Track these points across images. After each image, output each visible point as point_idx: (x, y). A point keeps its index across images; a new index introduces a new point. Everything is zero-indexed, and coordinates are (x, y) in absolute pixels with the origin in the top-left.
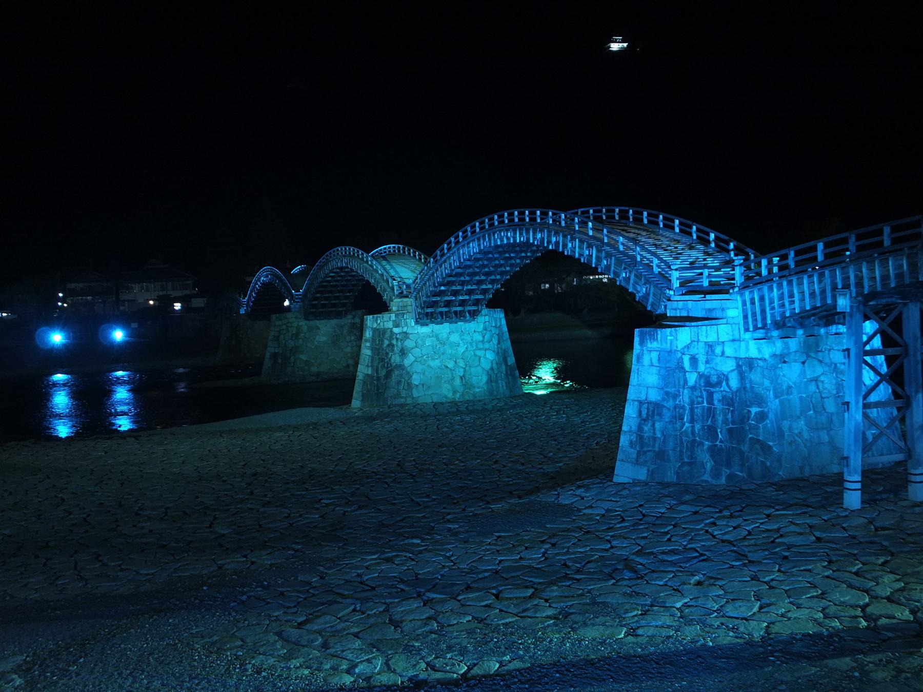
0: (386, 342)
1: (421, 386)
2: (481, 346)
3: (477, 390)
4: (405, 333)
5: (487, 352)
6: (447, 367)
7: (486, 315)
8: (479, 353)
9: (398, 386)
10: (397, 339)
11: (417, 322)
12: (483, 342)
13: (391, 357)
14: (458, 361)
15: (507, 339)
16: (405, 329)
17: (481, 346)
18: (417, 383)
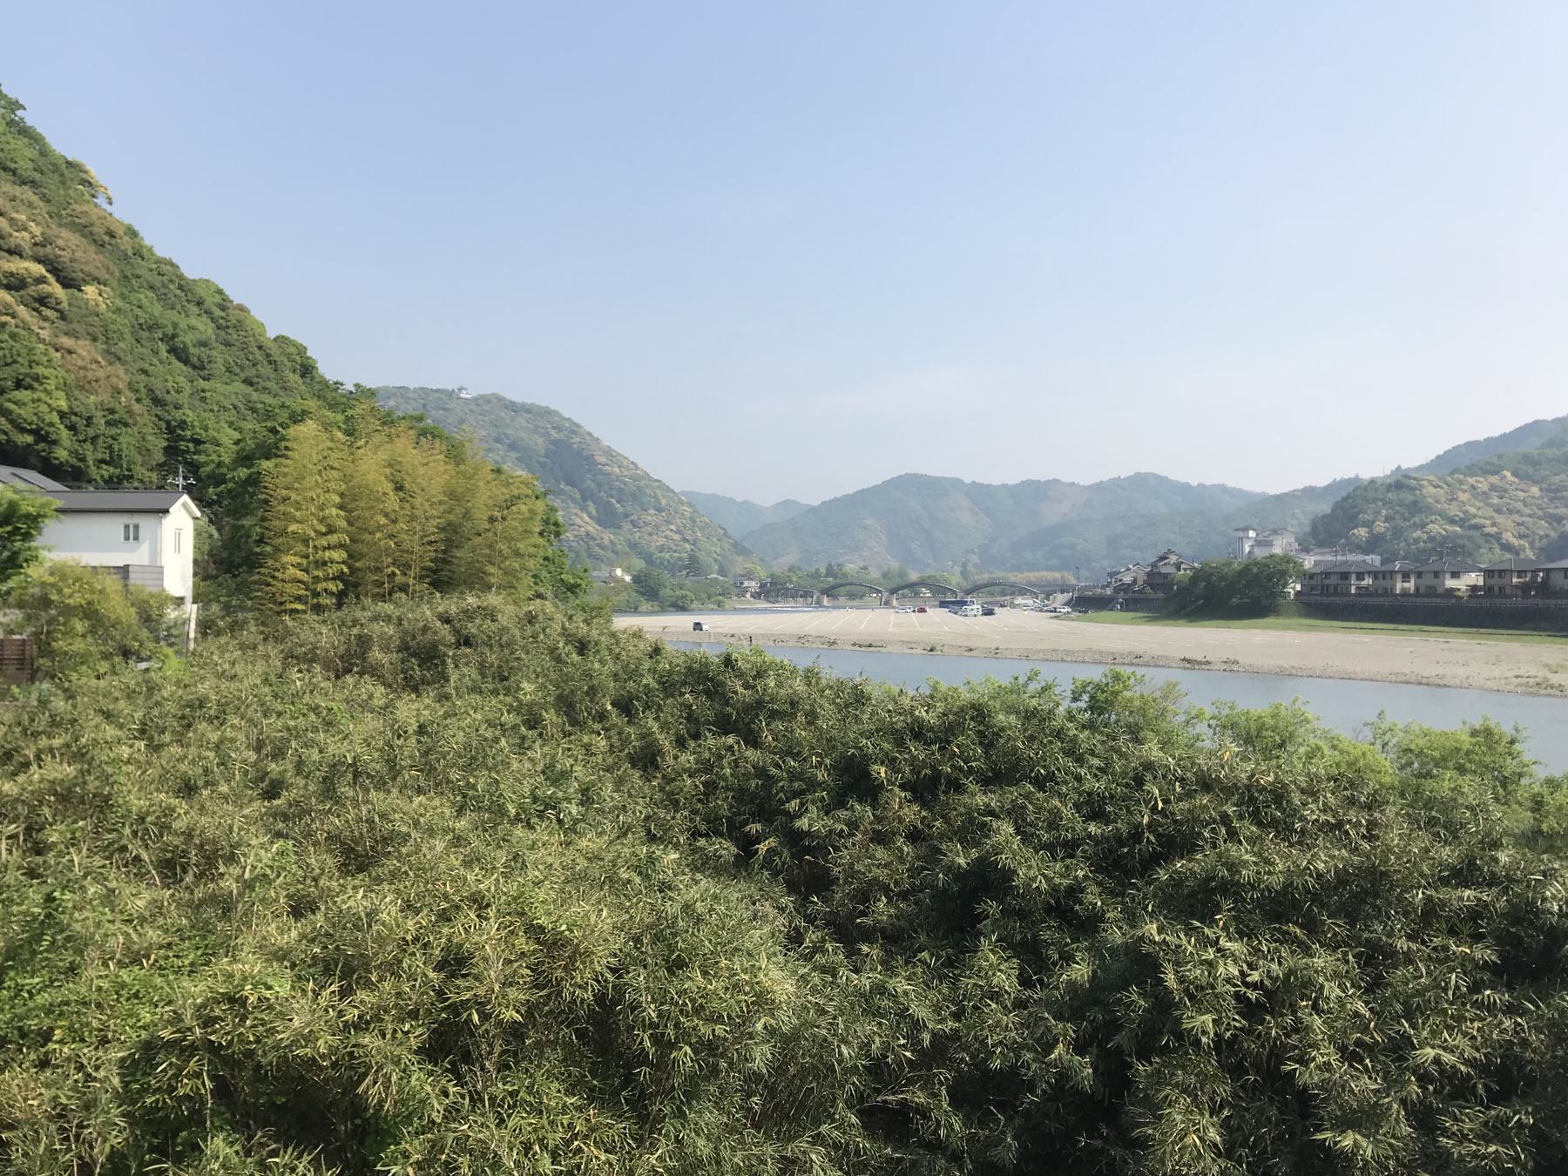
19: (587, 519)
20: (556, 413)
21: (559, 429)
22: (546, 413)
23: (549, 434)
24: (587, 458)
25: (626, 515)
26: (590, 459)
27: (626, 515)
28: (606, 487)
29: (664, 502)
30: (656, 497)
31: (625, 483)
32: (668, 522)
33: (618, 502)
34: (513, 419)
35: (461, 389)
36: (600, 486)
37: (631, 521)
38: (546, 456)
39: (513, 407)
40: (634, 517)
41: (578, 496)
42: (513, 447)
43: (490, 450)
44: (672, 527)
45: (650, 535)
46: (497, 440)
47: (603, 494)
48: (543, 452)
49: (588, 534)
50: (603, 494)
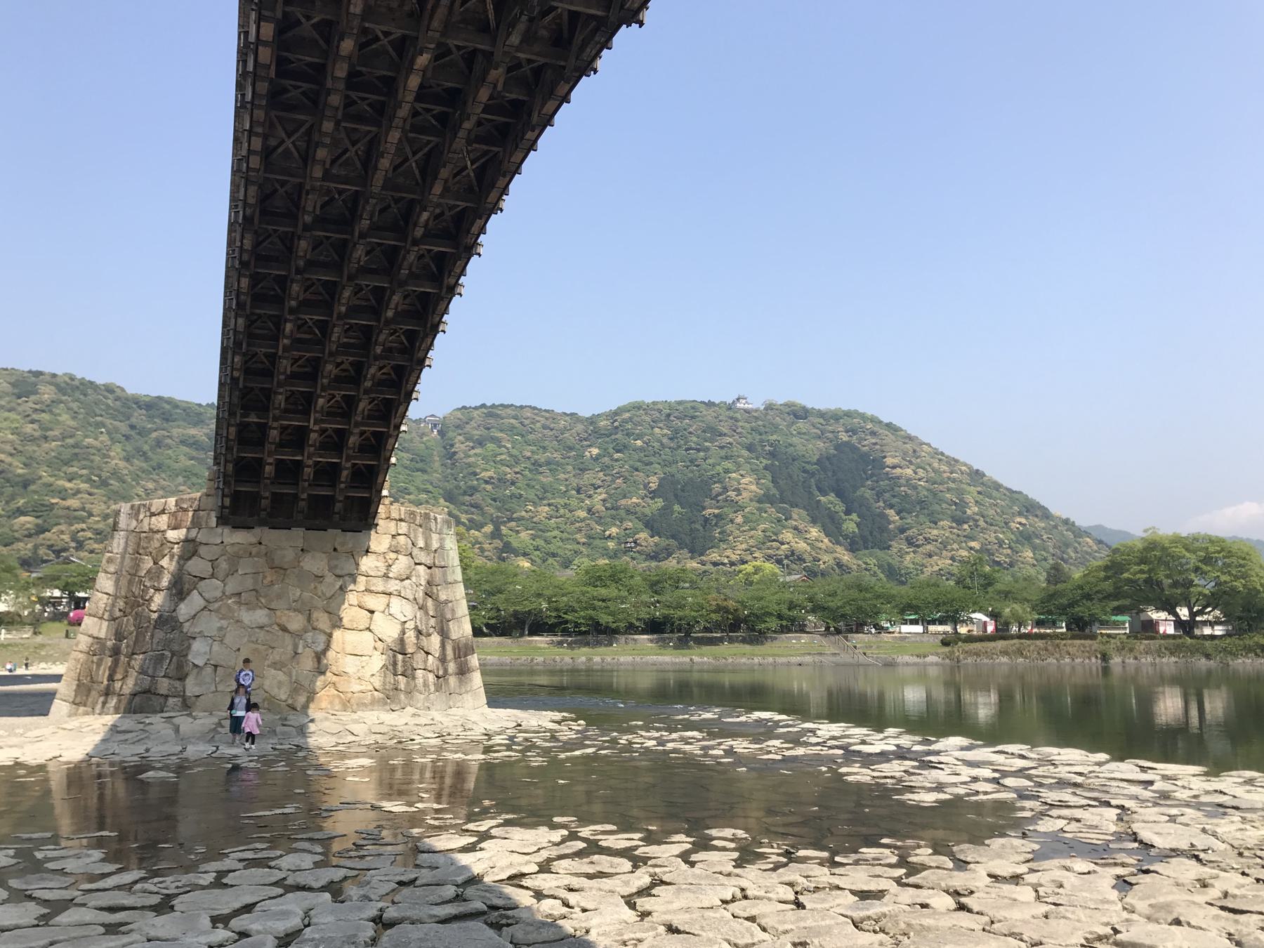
0: (148, 563)
1: (209, 670)
2: (379, 585)
3: (356, 687)
4: (193, 541)
5: (395, 602)
6: (284, 629)
7: (401, 520)
8: (371, 602)
9: (155, 669)
10: (171, 559)
11: (222, 520)
12: (386, 576)
13: (151, 597)
14: (315, 615)
15: (456, 582)
16: (193, 533)
17: (379, 585)
18: (200, 662)
19: (814, 532)
20: (863, 416)
21: (852, 431)
22: (848, 414)
23: (837, 438)
24: (873, 460)
25: (902, 531)
26: (879, 463)
27: (902, 531)
28: (887, 495)
29: (972, 510)
30: (961, 505)
31: (915, 488)
32: (973, 539)
33: (898, 514)
34: (793, 423)
35: (738, 399)
36: (879, 495)
37: (907, 539)
38: (819, 462)
39: (798, 413)
40: (909, 533)
41: (840, 507)
42: (772, 455)
43: (727, 458)
44: (973, 544)
45: (930, 556)
46: (750, 448)
47: (881, 504)
48: (815, 459)
49: (793, 553)
50: (881, 504)
